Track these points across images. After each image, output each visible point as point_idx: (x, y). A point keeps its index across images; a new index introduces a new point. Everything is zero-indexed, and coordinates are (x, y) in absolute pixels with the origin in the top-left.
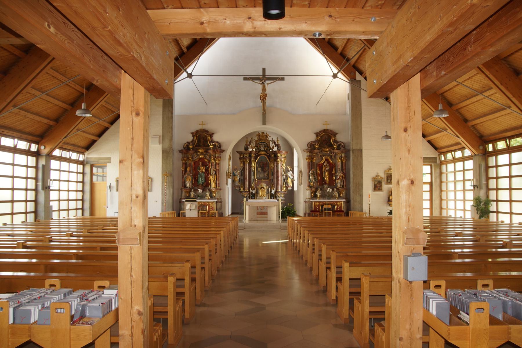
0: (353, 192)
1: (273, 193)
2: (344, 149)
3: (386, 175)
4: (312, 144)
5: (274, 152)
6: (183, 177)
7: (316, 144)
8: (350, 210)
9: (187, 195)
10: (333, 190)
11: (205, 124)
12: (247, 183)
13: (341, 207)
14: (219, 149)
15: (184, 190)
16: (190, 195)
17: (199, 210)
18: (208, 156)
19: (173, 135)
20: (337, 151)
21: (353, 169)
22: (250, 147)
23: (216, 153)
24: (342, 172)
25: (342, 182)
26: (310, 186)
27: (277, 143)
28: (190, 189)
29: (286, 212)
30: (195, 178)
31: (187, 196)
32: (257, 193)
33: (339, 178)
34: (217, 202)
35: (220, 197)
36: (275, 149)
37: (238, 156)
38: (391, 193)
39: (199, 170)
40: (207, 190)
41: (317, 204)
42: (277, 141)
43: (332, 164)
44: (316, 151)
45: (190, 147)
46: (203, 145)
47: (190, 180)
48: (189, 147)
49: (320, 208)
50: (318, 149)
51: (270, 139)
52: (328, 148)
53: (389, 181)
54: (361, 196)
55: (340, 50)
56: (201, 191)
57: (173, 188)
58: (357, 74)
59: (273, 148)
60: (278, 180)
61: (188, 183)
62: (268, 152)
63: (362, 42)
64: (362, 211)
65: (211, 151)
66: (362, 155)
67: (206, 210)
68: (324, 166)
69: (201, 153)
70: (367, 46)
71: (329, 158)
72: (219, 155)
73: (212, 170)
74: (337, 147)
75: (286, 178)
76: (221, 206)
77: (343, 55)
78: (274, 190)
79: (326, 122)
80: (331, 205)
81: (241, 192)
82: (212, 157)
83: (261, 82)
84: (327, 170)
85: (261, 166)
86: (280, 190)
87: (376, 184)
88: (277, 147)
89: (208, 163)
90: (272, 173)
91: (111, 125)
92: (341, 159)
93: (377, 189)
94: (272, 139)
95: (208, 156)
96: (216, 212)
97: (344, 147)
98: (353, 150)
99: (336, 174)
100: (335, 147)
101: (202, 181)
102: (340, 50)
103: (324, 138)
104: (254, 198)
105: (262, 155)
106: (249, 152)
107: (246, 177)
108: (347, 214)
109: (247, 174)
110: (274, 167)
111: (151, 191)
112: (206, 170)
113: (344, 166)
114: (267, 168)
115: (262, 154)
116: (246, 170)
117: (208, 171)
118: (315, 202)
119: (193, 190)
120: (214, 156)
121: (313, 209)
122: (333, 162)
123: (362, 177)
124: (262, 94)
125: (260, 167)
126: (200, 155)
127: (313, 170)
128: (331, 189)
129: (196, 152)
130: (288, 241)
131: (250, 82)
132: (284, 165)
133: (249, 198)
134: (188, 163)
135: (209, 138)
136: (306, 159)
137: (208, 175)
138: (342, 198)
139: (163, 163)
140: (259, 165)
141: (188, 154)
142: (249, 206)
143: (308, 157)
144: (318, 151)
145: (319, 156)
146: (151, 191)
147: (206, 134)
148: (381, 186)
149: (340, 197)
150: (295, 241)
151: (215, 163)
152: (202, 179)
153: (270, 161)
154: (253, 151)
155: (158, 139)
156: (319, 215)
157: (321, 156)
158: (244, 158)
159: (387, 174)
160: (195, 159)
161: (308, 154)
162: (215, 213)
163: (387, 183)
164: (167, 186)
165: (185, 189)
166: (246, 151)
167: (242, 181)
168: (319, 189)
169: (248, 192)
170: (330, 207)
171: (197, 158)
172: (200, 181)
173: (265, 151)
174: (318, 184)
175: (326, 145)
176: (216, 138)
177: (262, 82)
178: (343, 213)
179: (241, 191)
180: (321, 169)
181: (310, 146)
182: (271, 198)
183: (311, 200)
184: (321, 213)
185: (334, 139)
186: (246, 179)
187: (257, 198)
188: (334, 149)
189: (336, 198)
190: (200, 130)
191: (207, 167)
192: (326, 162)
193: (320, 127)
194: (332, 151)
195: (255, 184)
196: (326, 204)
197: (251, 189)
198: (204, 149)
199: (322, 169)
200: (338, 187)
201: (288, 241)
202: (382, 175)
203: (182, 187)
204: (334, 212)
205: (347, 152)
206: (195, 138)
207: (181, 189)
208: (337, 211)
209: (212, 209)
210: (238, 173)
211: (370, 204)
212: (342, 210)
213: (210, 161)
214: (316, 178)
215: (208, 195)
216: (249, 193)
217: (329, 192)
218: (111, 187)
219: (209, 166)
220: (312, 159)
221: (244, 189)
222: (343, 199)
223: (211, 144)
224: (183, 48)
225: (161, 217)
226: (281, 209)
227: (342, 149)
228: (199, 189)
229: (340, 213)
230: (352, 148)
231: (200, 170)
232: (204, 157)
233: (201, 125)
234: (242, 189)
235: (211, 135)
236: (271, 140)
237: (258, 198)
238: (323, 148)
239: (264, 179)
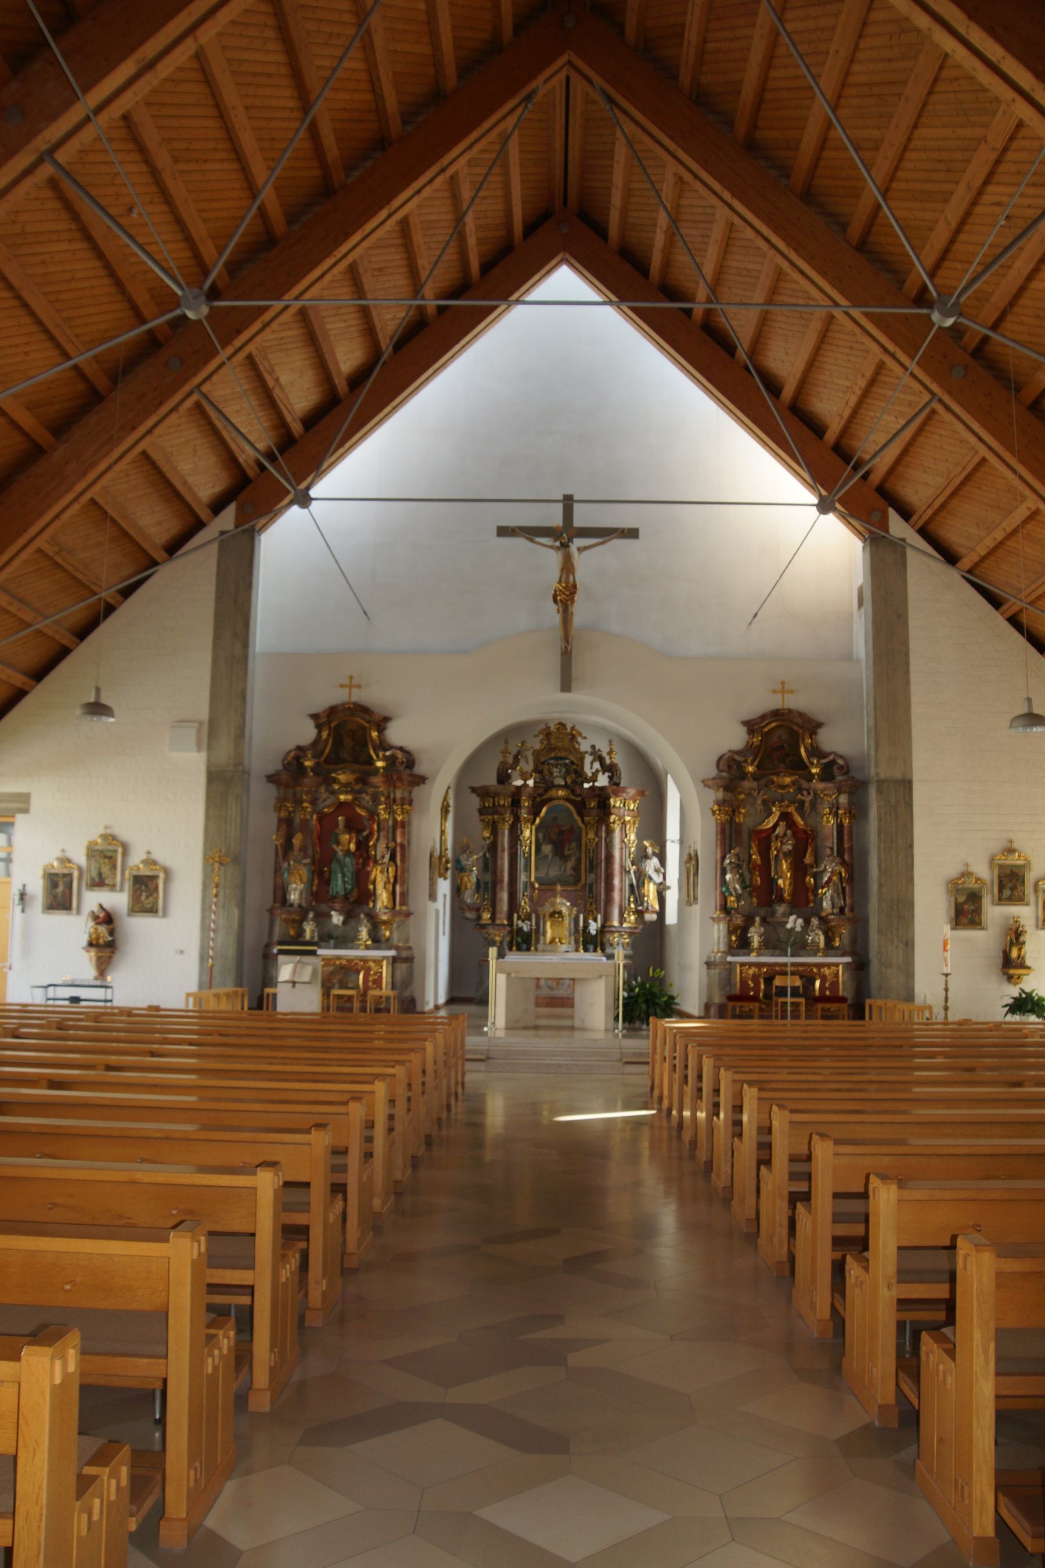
0: (880, 932)
1: (593, 932)
2: (845, 777)
3: (996, 872)
4: (734, 760)
5: (598, 792)
6: (277, 870)
7: (746, 761)
8: (869, 997)
9: (292, 932)
10: (807, 922)
11: (359, 686)
12: (504, 896)
13: (835, 984)
14: (408, 771)
15: (281, 916)
16: (301, 932)
17: (332, 987)
18: (367, 798)
19: (248, 718)
20: (821, 786)
21: (879, 848)
22: (515, 774)
23: (395, 787)
24: (838, 860)
25: (838, 894)
26: (725, 909)
27: (608, 761)
28: (303, 913)
29: (640, 1000)
30: (321, 873)
31: (292, 937)
32: (537, 931)
33: (830, 879)
34: (394, 960)
35: (407, 940)
36: (603, 781)
37: (475, 801)
38: (1015, 936)
39: (335, 847)
40: (362, 916)
41: (751, 972)
42: (610, 753)
43: (805, 832)
44: (747, 784)
45: (307, 763)
47: (302, 881)
48: (302, 764)
49: (762, 987)
50: (755, 777)
51: (584, 746)
52: (791, 775)
53: (1007, 893)
54: (907, 944)
55: (831, 436)
56: (341, 918)
57: (242, 904)
58: (893, 516)
59: (594, 779)
60: (609, 888)
61: (295, 889)
62: (578, 792)
63: (921, 388)
64: (910, 997)
65: (377, 780)
66: (911, 799)
67: (357, 987)
68: (777, 837)
69: (347, 785)
70: (940, 401)
71: (792, 809)
72: (406, 795)
73: (381, 847)
74: (822, 770)
75: (638, 881)
76: (410, 974)
77: (842, 451)
78: (595, 920)
79: (783, 683)
80: (801, 977)
81: (483, 927)
82: (383, 799)
83: (558, 544)
84: (785, 854)
85: (554, 837)
86: (616, 923)
87: (962, 904)
88: (607, 774)
89: (369, 820)
90: (591, 861)
91: (33, 683)
92: (836, 815)
93: (964, 920)
94: (593, 747)
95: (367, 798)
96: (391, 993)
97: (845, 770)
98: (880, 783)
99: (817, 867)
100: (814, 771)
101: (344, 882)
102: (831, 436)
103: (775, 739)
104: (528, 949)
105: (555, 802)
106: (512, 789)
107: (502, 876)
108: (858, 1011)
109: (503, 865)
110: (598, 844)
111: (165, 915)
112: (358, 845)
113: (846, 838)
114: (574, 845)
115: (558, 798)
116: (499, 849)
117: (367, 847)
118: (742, 965)
119: (311, 915)
120: (388, 797)
121: (737, 990)
122: (806, 824)
123: (910, 880)
124: (560, 582)
125: (551, 842)
126: (342, 793)
127: (737, 849)
128: (800, 921)
129: (329, 781)
130: (654, 1112)
131: (521, 542)
132: (633, 837)
133: (510, 949)
134: (297, 821)
135: (375, 734)
136: (714, 813)
137: (365, 864)
138: (840, 952)
139: (208, 817)
140: (544, 838)
141: (298, 789)
142: (509, 975)
143: (721, 803)
144: (754, 784)
145: (759, 801)
146: (165, 915)
147: (363, 719)
148: (978, 911)
149: (833, 948)
150: (687, 1114)
151: (391, 823)
152: (344, 876)
153: (583, 821)
154: (525, 785)
155: (193, 732)
156: (757, 1013)
157: (764, 802)
158: (495, 810)
159: (1001, 867)
160: (321, 805)
161: (720, 795)
162: (388, 998)
163: (1000, 899)
164: (221, 894)
165: (286, 909)
166: (501, 786)
167: (486, 889)
168: (758, 919)
169: (508, 929)
170: (798, 983)
171: (328, 802)
172: (339, 884)
173: (565, 787)
174: (754, 900)
175: (782, 765)
176: (397, 734)
177: (562, 544)
178: (845, 1006)
179: (483, 922)
180: (765, 851)
181: (726, 768)
182: (586, 950)
183: (729, 959)
184: (763, 1006)
185: (811, 744)
186: (502, 881)
187: (536, 950)
188: (810, 777)
189: (818, 950)
190: (343, 704)
191: (365, 833)
192: (782, 824)
193: (761, 702)
194: (805, 784)
195: (531, 899)
196: (785, 974)
197: (515, 916)
198: (353, 772)
199: (769, 848)
200: (824, 914)
201: (654, 1112)
202: (983, 871)
203: (275, 901)
204: (813, 1000)
205: (857, 788)
206: (325, 734)
207: (271, 911)
208: (823, 999)
209: (378, 982)
210: (473, 863)
211: (947, 975)
212: (841, 994)
213: (373, 814)
214: (748, 883)
215: (364, 933)
216: (511, 932)
217: (793, 929)
218: (26, 898)
219: (371, 833)
220: (734, 811)
221: (493, 917)
222: (843, 955)
223: (378, 756)
224: (289, 419)
225: (191, 1007)
226: (624, 990)
227: (840, 778)
228: (333, 913)
229: (834, 1007)
230: (877, 774)
231: (338, 843)
232: (355, 799)
233: (347, 690)
234: (486, 916)
235: (382, 723)
236: (590, 750)
237: (540, 947)
238: (774, 774)
239: (564, 883)
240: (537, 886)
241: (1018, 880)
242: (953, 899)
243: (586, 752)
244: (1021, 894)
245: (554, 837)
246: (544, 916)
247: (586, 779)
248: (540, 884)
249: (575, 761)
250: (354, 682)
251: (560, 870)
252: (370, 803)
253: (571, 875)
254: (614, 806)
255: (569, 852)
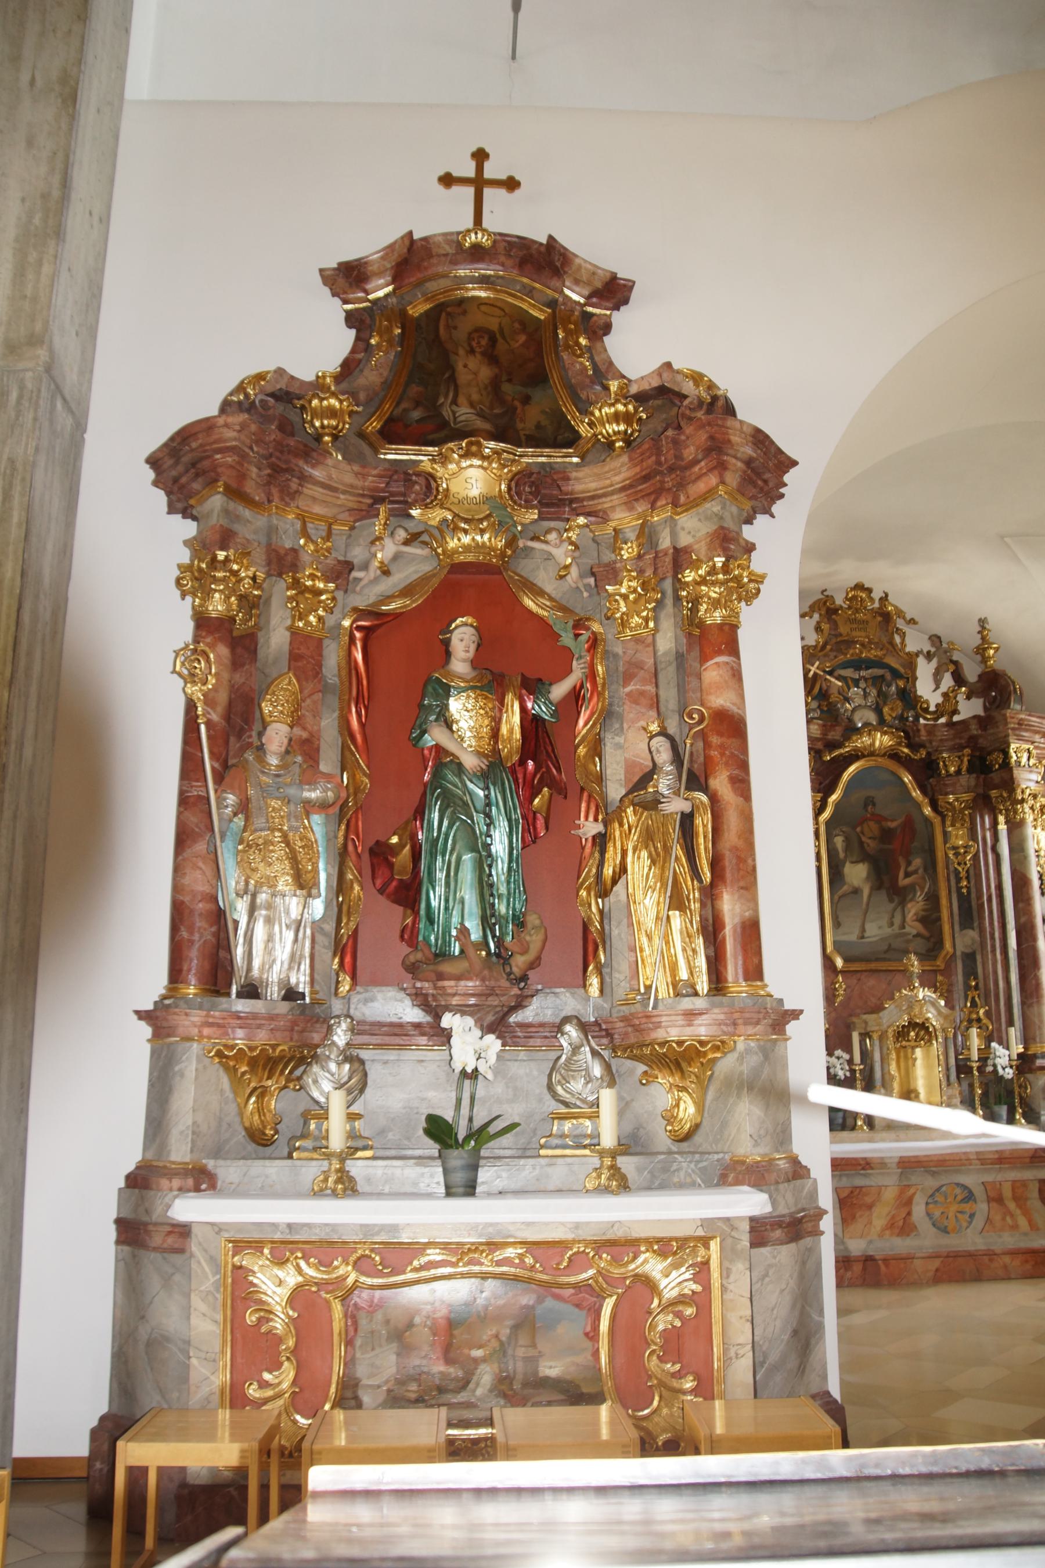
1: (1009, 1073)
19: (83, 180)
46: (480, 424)
85: (872, 845)
90: (965, 901)
114: (917, 862)
125: (865, 857)
140: (848, 848)
171: (401, 577)
203: (176, 974)
233: (470, 172)
236: (927, 647)
240: (839, 963)
243: (917, 655)
245: (872, 845)
246: (882, 1037)
247: (926, 710)
248: (846, 960)
249: (902, 670)
250: (491, 171)
251: (891, 924)
252: (574, 572)
253: (918, 935)
254: (1018, 763)
255: (908, 881)
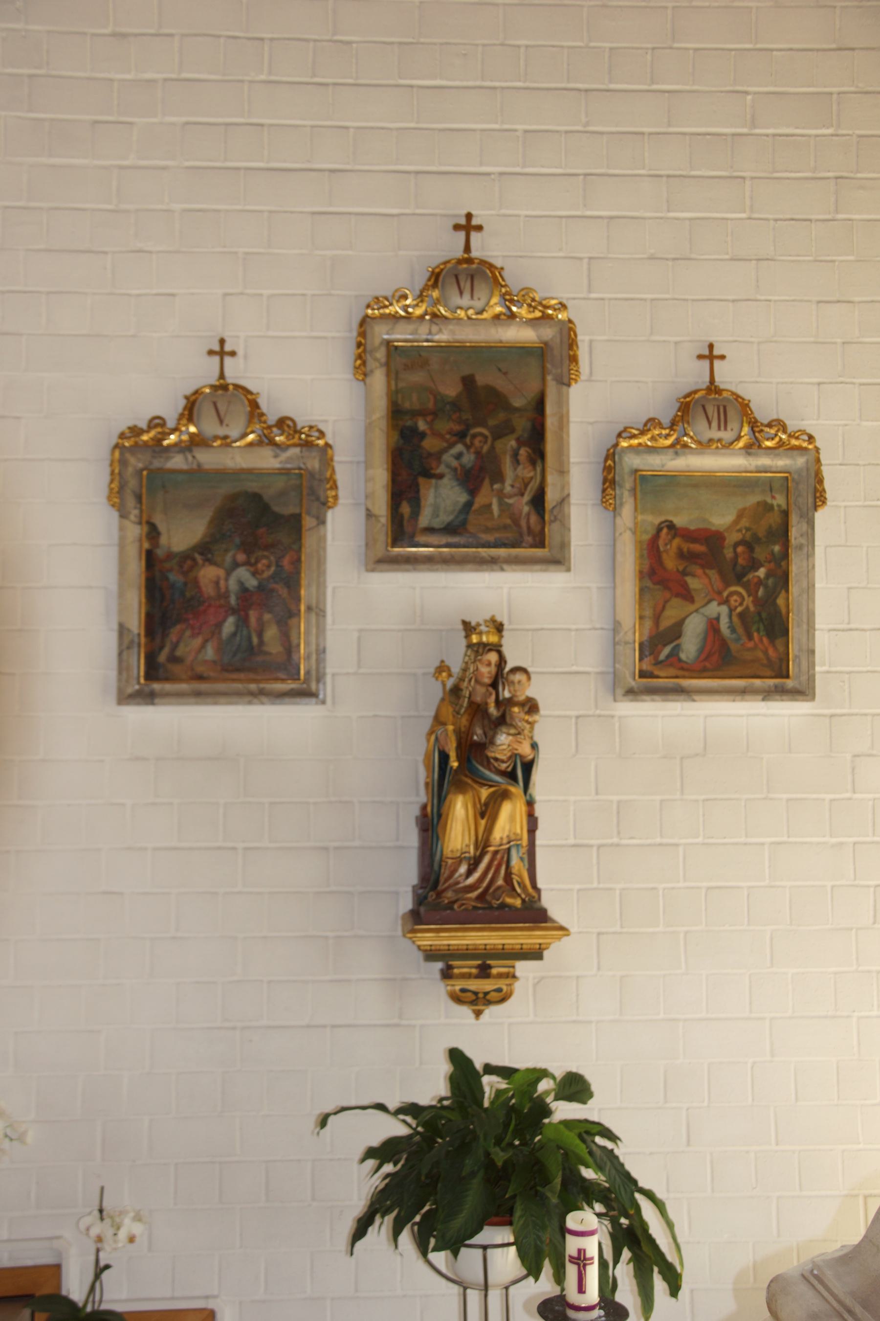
3: (379, 380)
241: (499, 433)
242: (134, 531)
244: (523, 505)
